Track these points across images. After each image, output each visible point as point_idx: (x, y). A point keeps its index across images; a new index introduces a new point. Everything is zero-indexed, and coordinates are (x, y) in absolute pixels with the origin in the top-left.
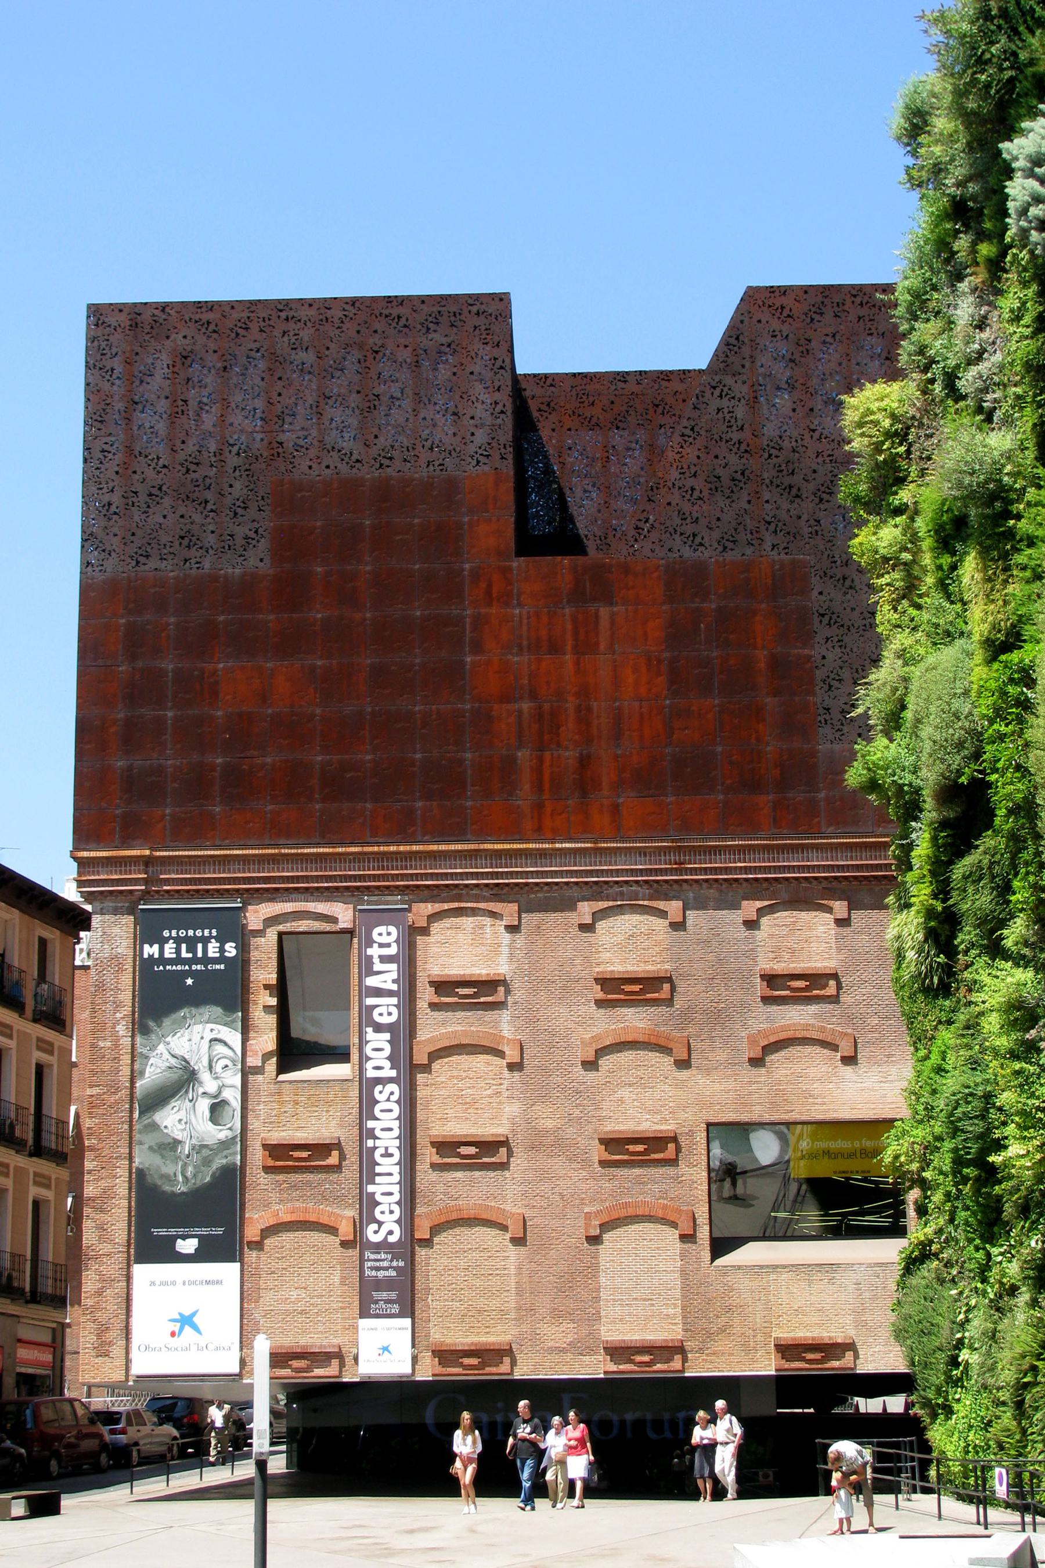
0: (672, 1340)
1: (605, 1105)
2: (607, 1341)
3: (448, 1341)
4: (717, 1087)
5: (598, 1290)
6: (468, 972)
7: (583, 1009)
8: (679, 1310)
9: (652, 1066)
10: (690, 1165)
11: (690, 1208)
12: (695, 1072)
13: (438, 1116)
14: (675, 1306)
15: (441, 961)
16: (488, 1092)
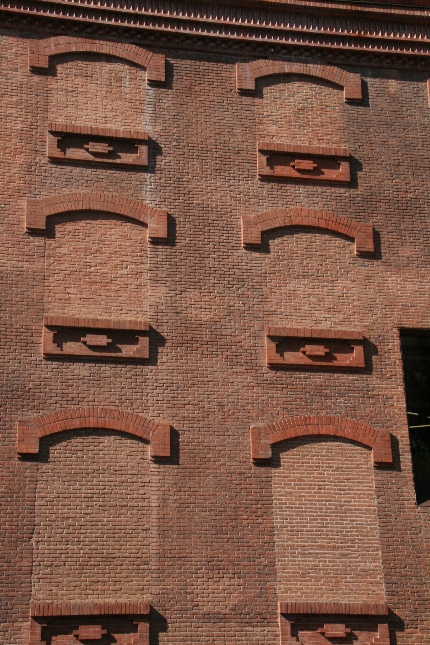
0: (376, 606)
1: (272, 298)
2: (287, 605)
3: (58, 602)
4: (409, 286)
5: (271, 532)
6: (101, 126)
7: (244, 186)
8: (379, 563)
9: (330, 257)
10: (382, 376)
11: (385, 429)
12: (381, 268)
13: (58, 296)
14: (375, 558)
15: (66, 112)
16: (125, 271)
